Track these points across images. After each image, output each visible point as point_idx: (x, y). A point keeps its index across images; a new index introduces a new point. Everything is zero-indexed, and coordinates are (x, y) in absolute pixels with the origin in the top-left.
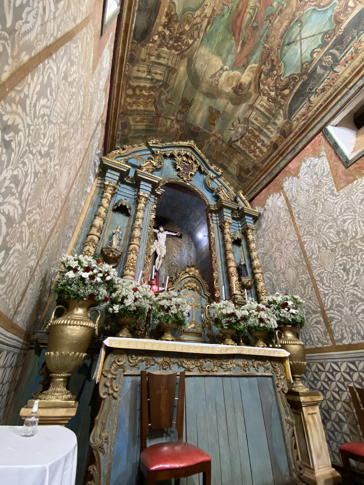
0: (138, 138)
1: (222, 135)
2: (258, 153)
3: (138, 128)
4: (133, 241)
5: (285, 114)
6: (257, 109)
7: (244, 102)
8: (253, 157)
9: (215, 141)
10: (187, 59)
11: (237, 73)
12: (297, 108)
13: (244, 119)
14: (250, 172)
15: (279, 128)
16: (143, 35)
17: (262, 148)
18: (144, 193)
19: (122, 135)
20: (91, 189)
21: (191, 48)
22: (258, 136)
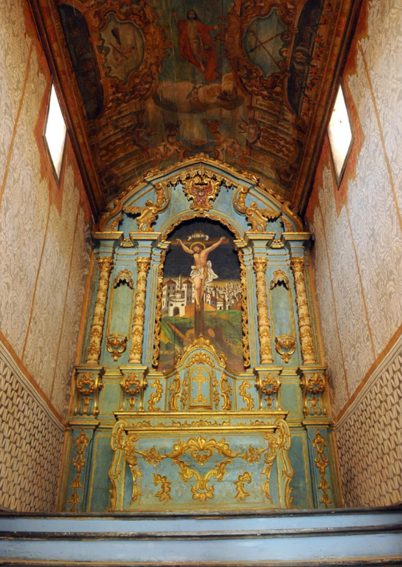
0: (130, 179)
1: (234, 139)
2: (286, 152)
3: (127, 171)
4: (135, 322)
5: (290, 110)
6: (258, 109)
7: (240, 105)
8: (284, 157)
9: (231, 147)
10: (151, 98)
11: (213, 85)
12: (299, 104)
13: (250, 119)
14: (290, 175)
15: (292, 124)
16: (98, 112)
17: (288, 146)
18: (143, 258)
19: (110, 187)
20: (89, 269)
21: (151, 89)
22: (276, 134)
